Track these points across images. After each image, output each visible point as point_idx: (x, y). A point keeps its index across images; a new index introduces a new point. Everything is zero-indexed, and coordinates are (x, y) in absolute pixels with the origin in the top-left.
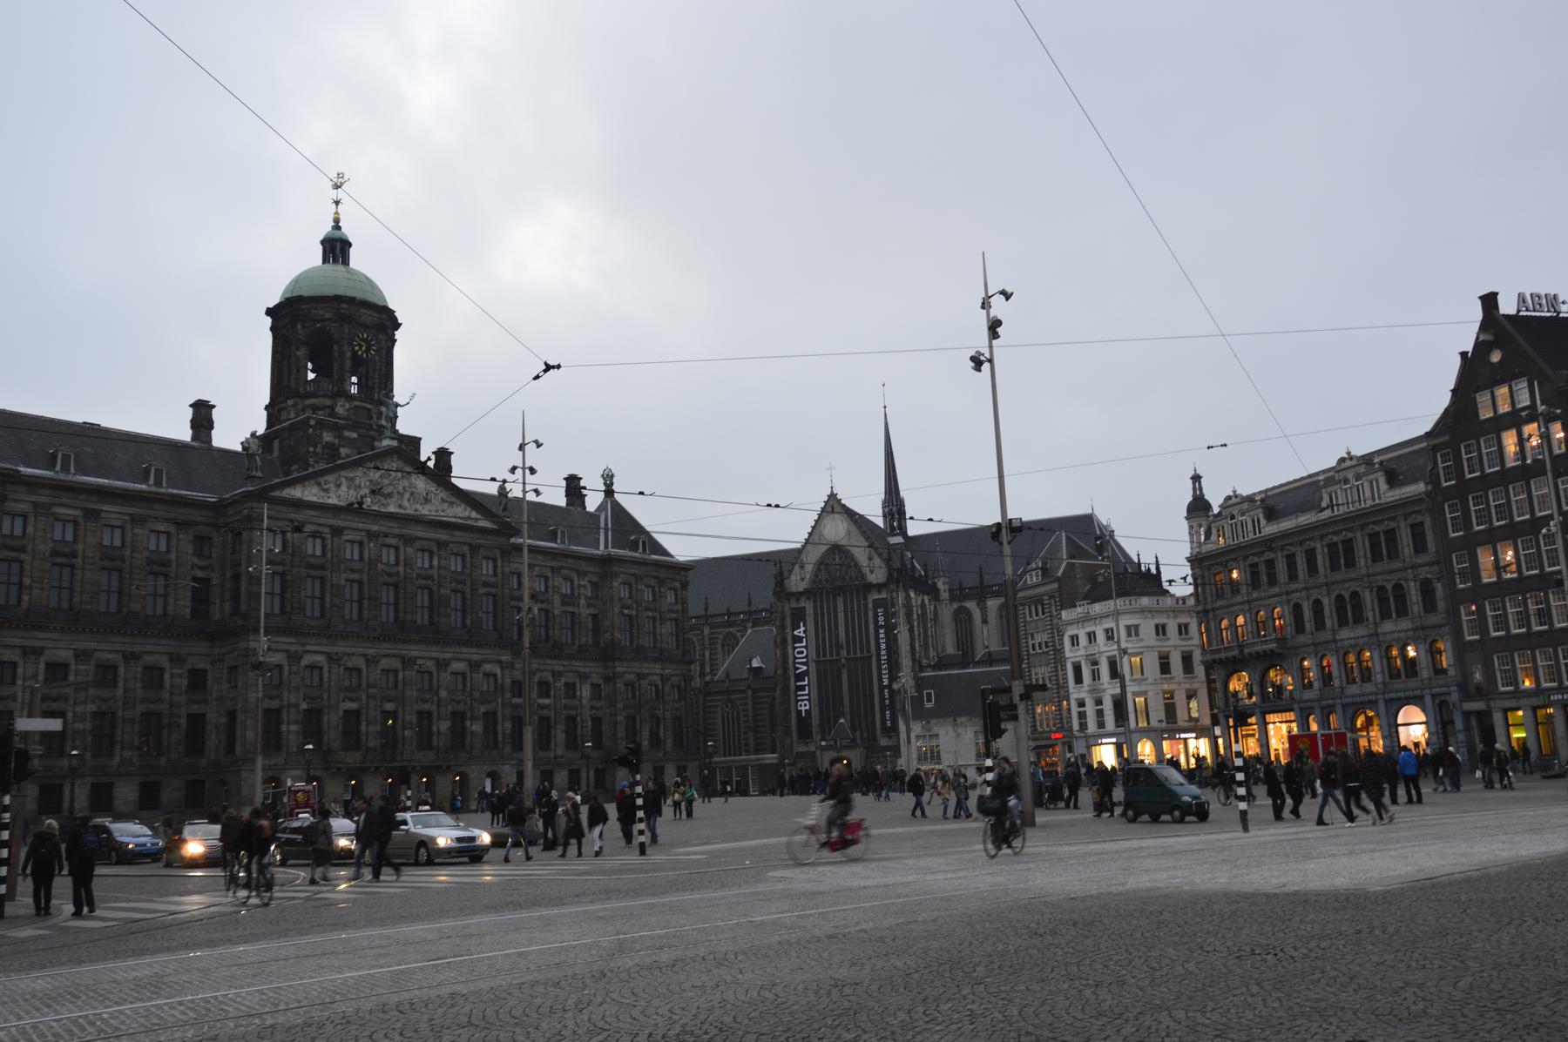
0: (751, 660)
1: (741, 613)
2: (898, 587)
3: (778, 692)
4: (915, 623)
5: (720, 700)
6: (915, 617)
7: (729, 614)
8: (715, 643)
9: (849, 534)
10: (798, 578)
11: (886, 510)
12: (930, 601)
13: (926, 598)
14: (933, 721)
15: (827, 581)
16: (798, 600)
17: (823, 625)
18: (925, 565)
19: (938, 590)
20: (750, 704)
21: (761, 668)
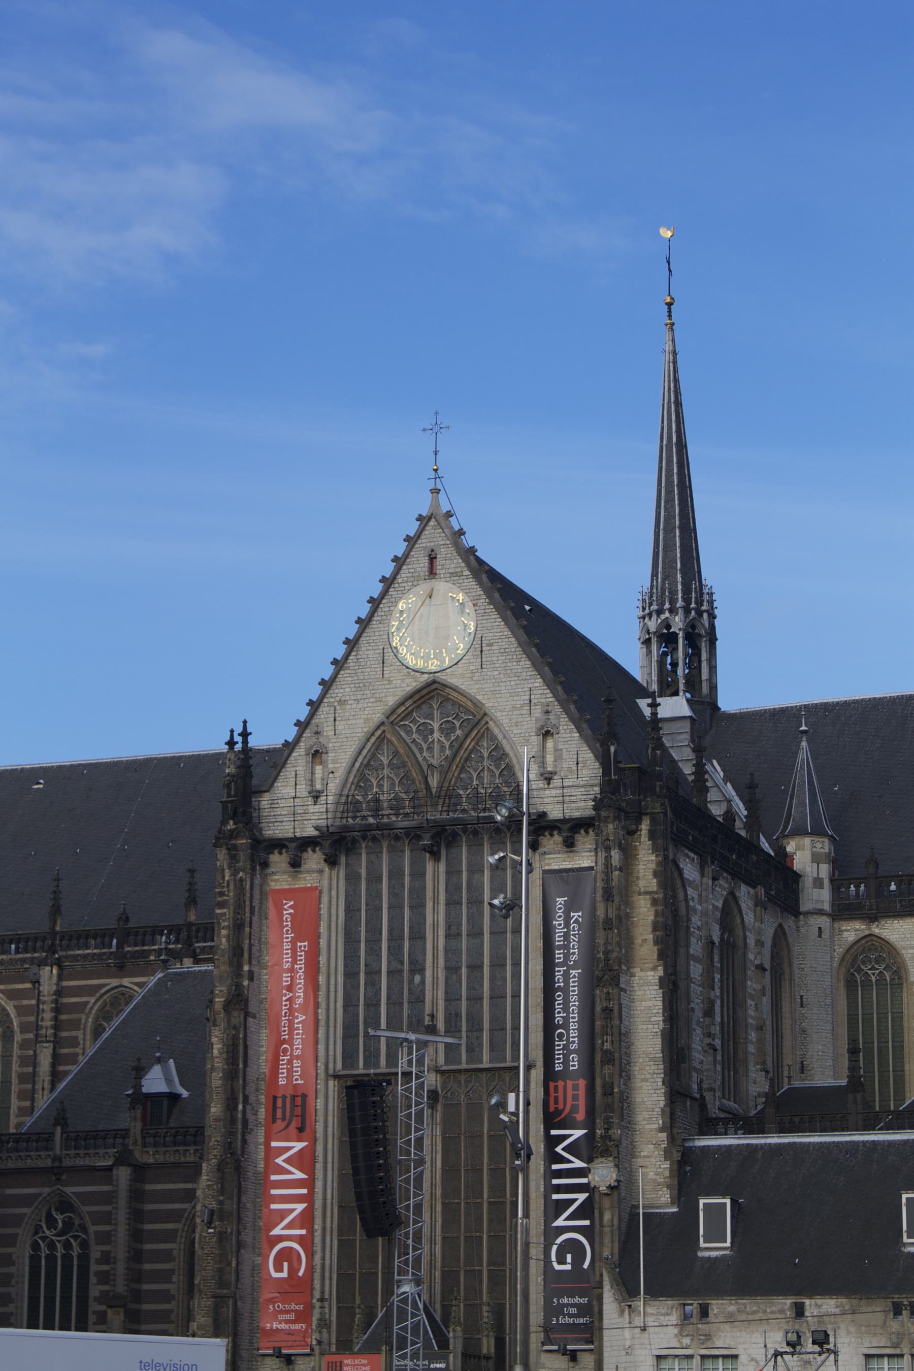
0: (140, 1071)
1: (157, 931)
2: (632, 833)
3: (205, 1178)
4: (696, 970)
5: (27, 1201)
6: (696, 948)
7: (126, 934)
8: (75, 1025)
9: (479, 646)
10: (303, 790)
11: (653, 624)
12: (758, 903)
13: (744, 893)
14: (718, 1307)
15: (396, 807)
16: (296, 864)
18: (752, 787)
19: (796, 877)
20: (122, 1216)
21: (173, 1097)
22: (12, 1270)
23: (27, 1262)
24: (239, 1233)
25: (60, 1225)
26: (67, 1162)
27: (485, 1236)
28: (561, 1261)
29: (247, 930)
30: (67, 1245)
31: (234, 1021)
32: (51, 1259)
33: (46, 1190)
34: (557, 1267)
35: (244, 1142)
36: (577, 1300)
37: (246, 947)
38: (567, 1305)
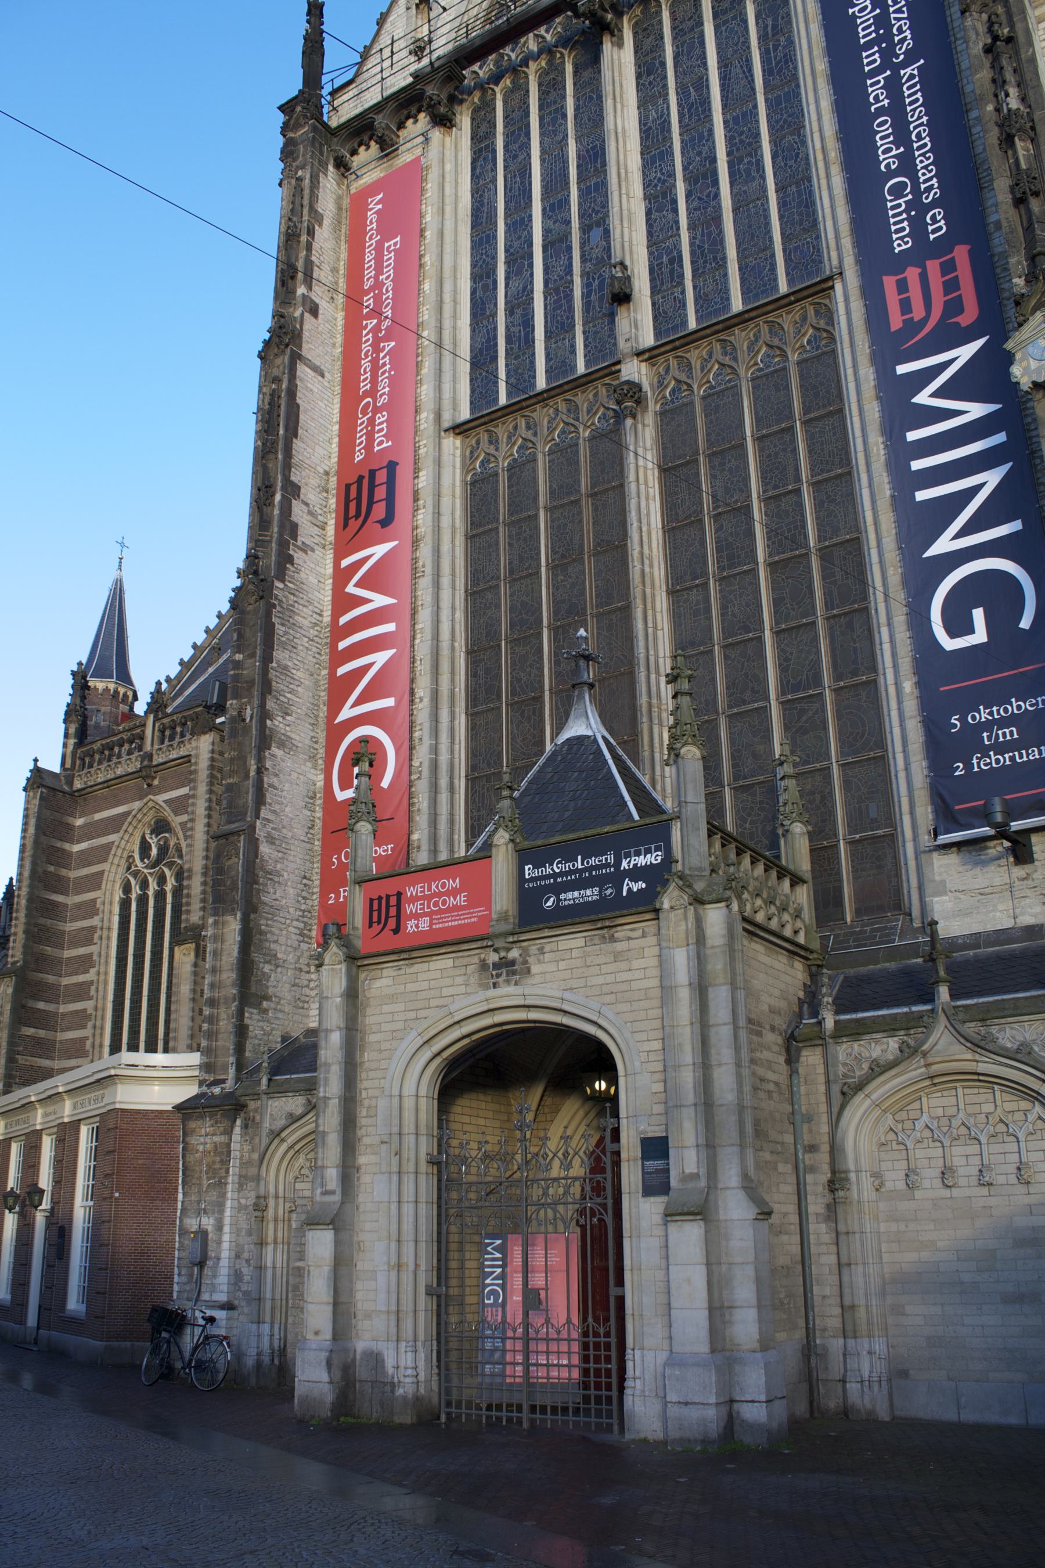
17: (519, 225)
22: (95, 921)
23: (116, 909)
24: (264, 715)
25: (154, 851)
26: (157, 760)
27: (768, 633)
28: (957, 625)
29: (304, 238)
30: (162, 880)
31: (276, 372)
32: (143, 900)
33: (137, 805)
34: (949, 644)
35: (286, 559)
36: (1015, 706)
37: (300, 265)
38: (988, 726)
